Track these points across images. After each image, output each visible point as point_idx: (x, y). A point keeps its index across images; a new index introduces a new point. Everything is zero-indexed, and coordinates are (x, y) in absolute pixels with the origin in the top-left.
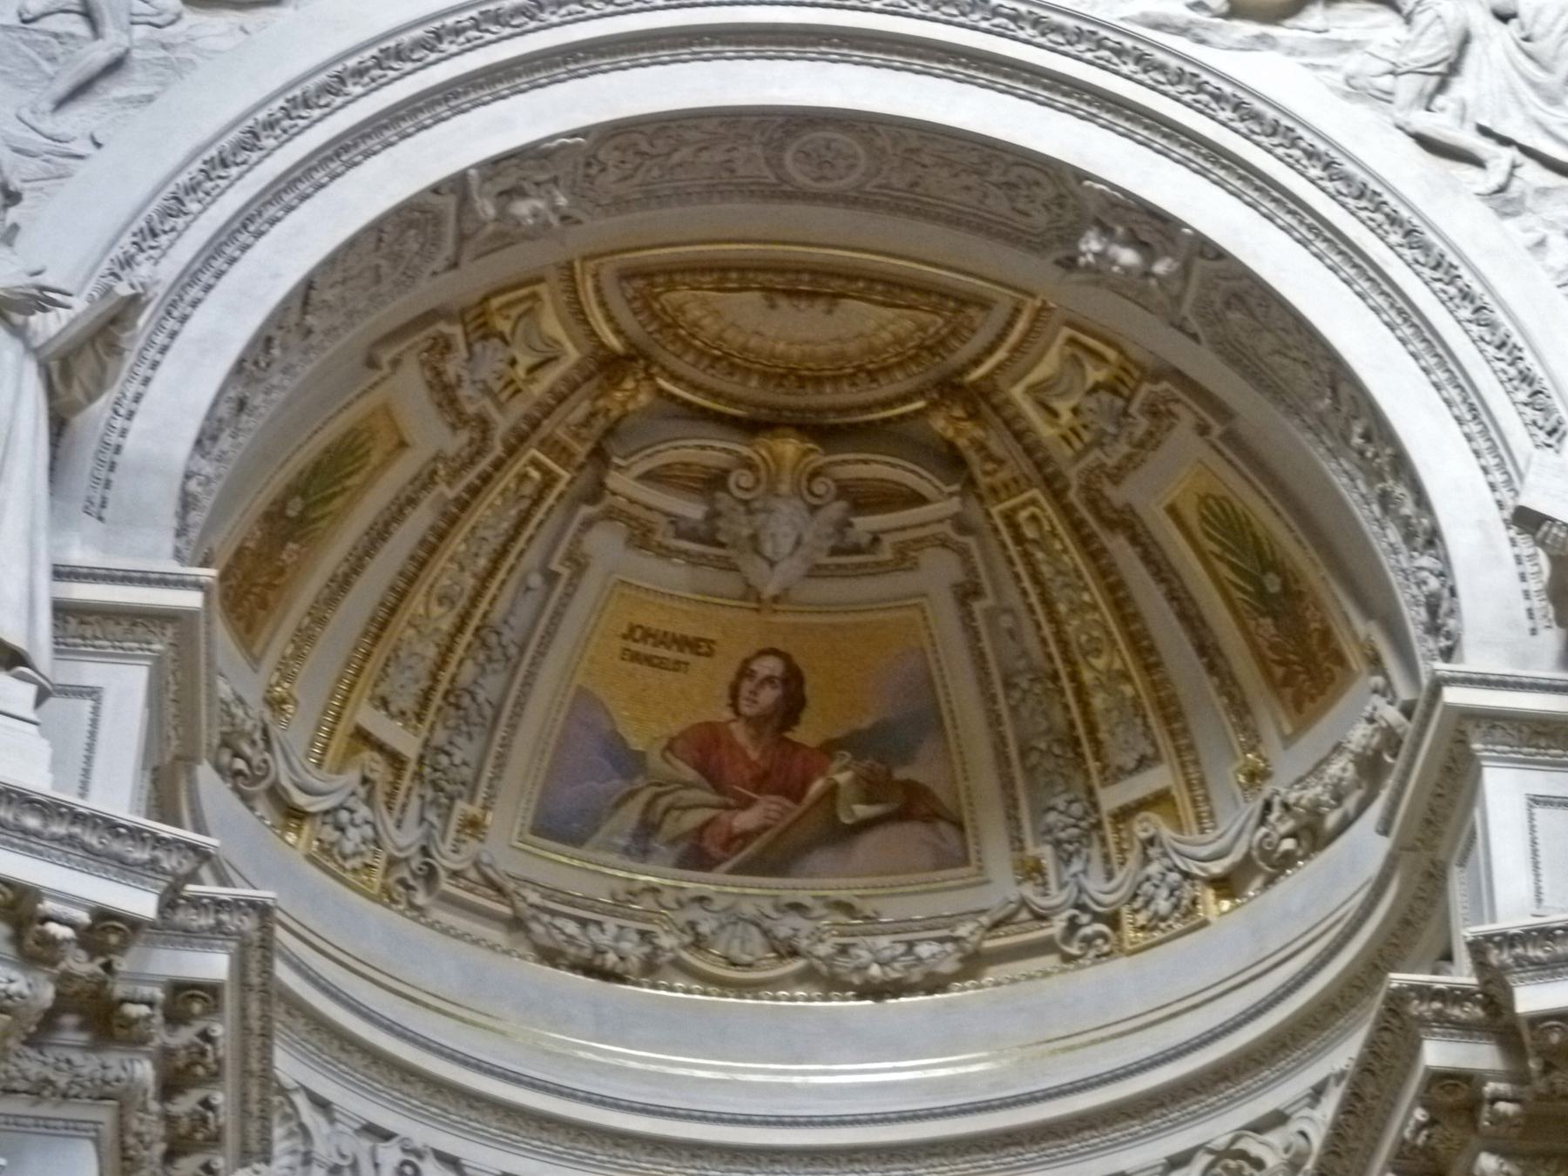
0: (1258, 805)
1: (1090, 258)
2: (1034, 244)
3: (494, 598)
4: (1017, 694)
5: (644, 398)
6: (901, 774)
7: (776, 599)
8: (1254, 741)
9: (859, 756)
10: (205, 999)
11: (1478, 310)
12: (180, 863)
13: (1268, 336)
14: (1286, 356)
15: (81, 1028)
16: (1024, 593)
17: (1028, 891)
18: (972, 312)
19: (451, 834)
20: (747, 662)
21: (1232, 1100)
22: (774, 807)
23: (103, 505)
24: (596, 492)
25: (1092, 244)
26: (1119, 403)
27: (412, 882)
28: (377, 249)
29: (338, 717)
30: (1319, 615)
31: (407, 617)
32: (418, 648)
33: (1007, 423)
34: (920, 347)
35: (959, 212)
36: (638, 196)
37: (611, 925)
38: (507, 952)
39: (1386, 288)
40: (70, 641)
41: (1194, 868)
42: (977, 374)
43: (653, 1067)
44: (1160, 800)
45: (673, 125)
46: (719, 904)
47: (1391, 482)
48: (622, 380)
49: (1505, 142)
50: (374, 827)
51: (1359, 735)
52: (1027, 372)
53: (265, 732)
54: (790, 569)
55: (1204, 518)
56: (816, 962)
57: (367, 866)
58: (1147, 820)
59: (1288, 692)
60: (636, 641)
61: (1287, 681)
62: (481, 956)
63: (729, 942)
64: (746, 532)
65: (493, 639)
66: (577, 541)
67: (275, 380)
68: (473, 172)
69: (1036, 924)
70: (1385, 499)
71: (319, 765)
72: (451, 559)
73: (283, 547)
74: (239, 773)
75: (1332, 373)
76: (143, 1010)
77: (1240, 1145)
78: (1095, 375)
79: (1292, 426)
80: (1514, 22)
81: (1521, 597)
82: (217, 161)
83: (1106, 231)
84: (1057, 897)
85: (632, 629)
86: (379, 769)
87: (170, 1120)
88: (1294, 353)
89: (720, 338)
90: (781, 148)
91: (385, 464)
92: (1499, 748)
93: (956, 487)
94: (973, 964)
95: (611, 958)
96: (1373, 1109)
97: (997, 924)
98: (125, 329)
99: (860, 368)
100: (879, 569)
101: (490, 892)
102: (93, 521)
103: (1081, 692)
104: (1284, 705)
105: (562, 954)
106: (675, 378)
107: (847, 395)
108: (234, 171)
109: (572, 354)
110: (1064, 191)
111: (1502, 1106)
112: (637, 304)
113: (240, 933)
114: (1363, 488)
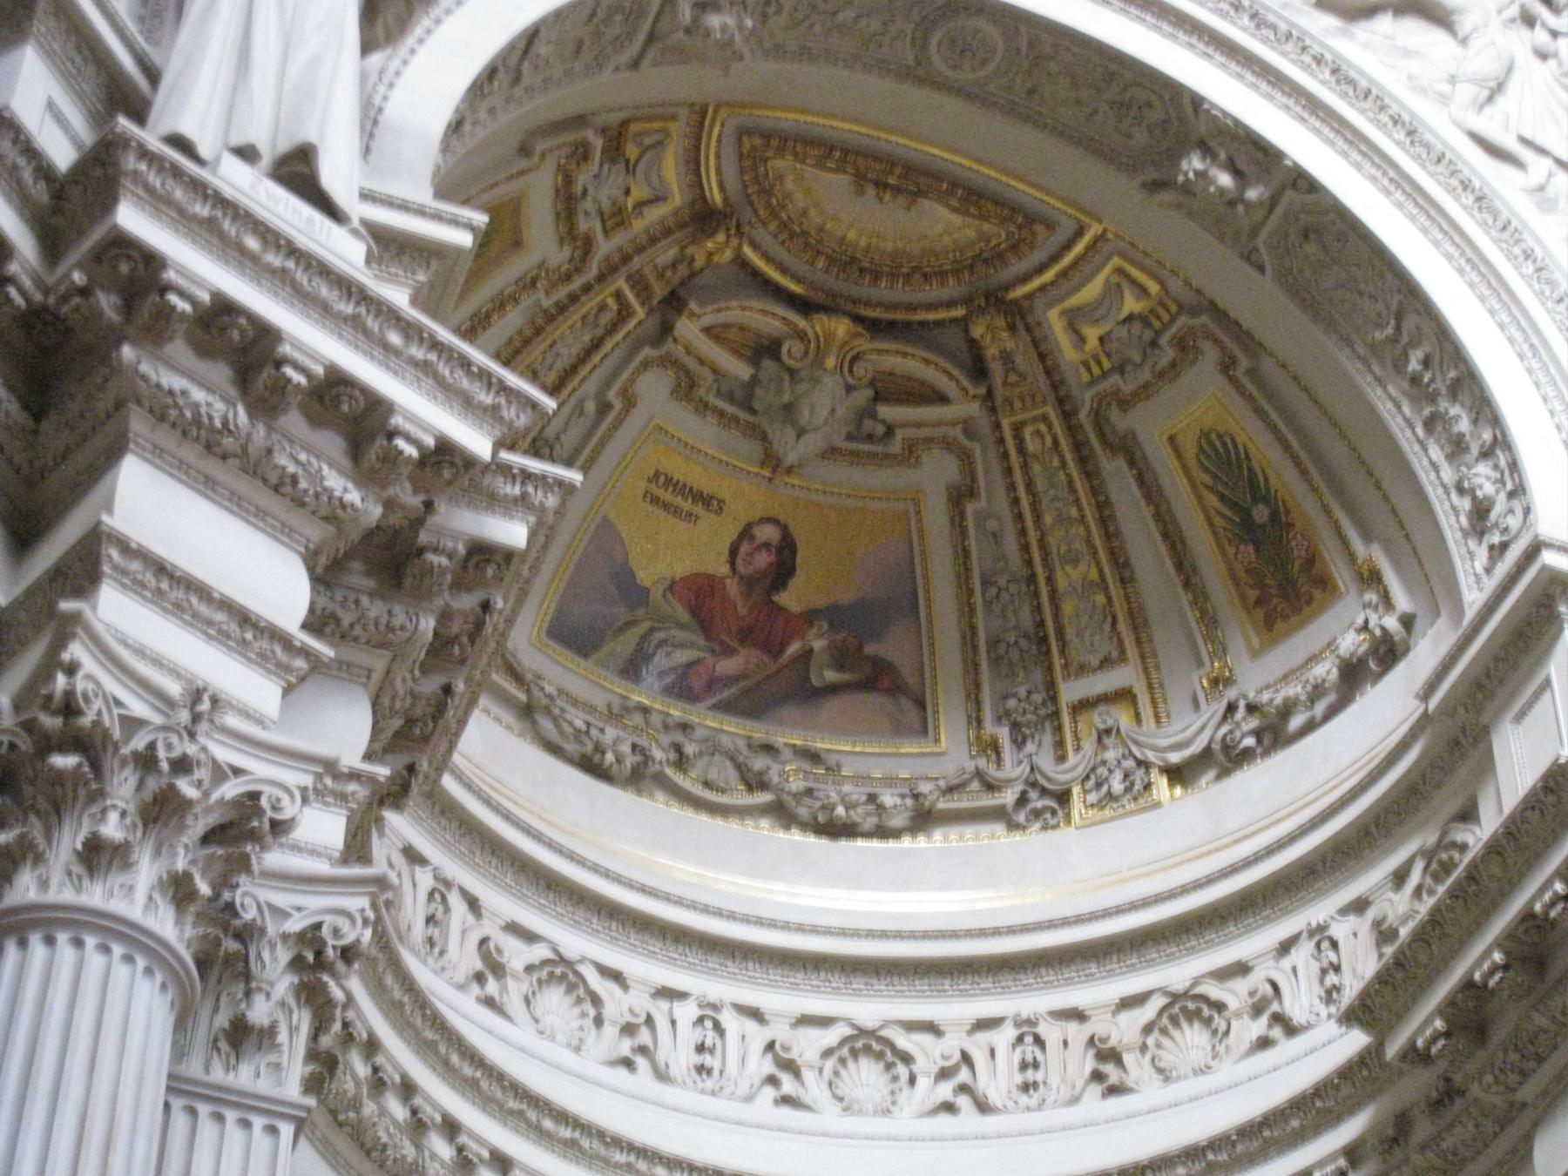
4: (993, 591)
5: (728, 255)
6: (870, 649)
8: (1221, 651)
11: (1539, 270)
15: (368, 573)
16: (1016, 501)
18: (1039, 228)
24: (666, 329)
25: (1195, 163)
33: (1035, 343)
41: (1151, 756)
42: (1020, 291)
48: (715, 231)
49: (1542, 151)
51: (1350, 643)
52: (1069, 294)
54: (812, 443)
56: (785, 796)
59: (1260, 613)
66: (632, 381)
76: (444, 561)
77: (1199, 990)
78: (1131, 304)
79: (1343, 356)
80: (1552, 63)
83: (1207, 150)
85: (657, 474)
94: (923, 819)
97: (950, 790)
99: (915, 269)
100: (887, 459)
106: (755, 246)
113: (542, 509)
114: (1407, 410)
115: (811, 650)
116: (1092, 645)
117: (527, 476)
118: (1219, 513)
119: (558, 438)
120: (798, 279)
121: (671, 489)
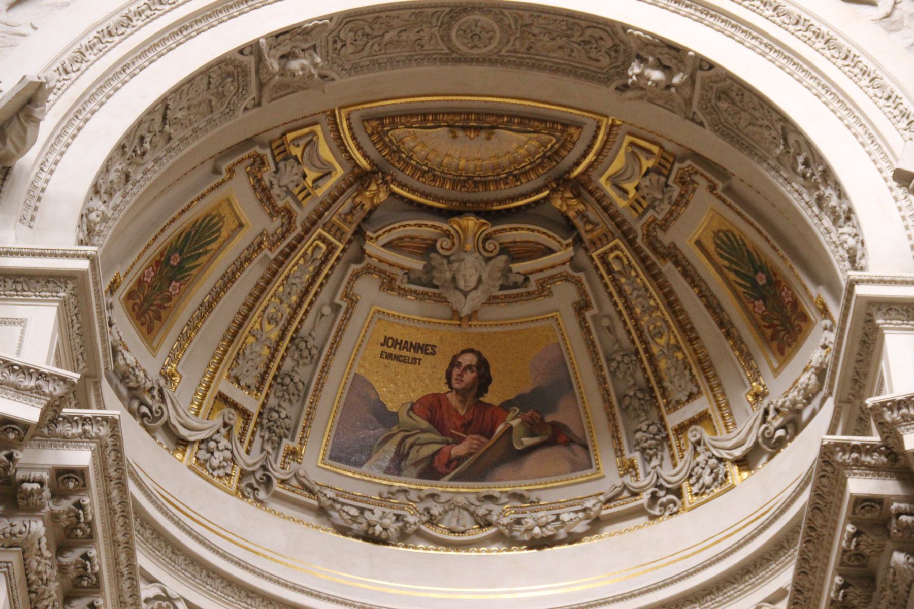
0: (761, 412)
1: (634, 78)
2: (603, 79)
3: (302, 321)
4: (614, 364)
5: (383, 196)
6: (549, 419)
7: (470, 317)
8: (756, 375)
9: (524, 409)
10: (76, 480)
12: (55, 389)
13: (743, 114)
14: (754, 125)
16: (615, 304)
17: (628, 479)
18: (572, 130)
19: (280, 458)
20: (455, 357)
21: (754, 585)
22: (476, 442)
23: (33, 219)
25: (635, 69)
26: (663, 179)
27: (256, 486)
28: (209, 88)
29: (208, 387)
30: (790, 293)
31: (248, 329)
32: (257, 348)
33: (599, 201)
34: (544, 157)
35: (558, 64)
36: (368, 63)
37: (378, 511)
38: (317, 528)
39: (814, 74)
40: (7, 293)
41: (724, 454)
43: (405, 592)
44: (703, 418)
45: (383, 15)
46: (443, 498)
47: (822, 188)
48: (368, 186)
50: (232, 452)
53: (161, 391)
54: (477, 298)
55: (717, 245)
57: (227, 475)
58: (695, 430)
59: (775, 344)
60: (388, 346)
61: (773, 338)
62: (300, 528)
63: (450, 520)
64: (449, 275)
65: (303, 345)
67: (150, 166)
68: (262, 41)
69: (633, 499)
70: (820, 201)
71: (197, 414)
72: (274, 295)
73: (170, 284)
74: (144, 415)
75: (783, 129)
78: (647, 164)
79: (762, 169)
81: (906, 238)
82: (105, 32)
83: (642, 60)
84: (644, 481)
85: (386, 340)
86: (237, 422)
87: (62, 569)
88: (760, 122)
89: (426, 159)
90: (449, 28)
91: (230, 238)
92: (894, 322)
93: (570, 240)
94: (597, 524)
95: (378, 529)
96: (823, 535)
97: (609, 501)
98: (37, 106)
99: (510, 173)
100: (530, 296)
101: (305, 493)
102: (26, 228)
103: (652, 359)
104: (773, 352)
105: (351, 529)
106: (402, 185)
107: (505, 191)
108: (117, 39)
109: (339, 172)
110: (617, 41)
111: (904, 518)
112: (375, 138)
114: (805, 196)
115: (511, 427)
116: (681, 386)
117: (85, 420)
118: (739, 284)
119: (310, 335)
120: (436, 199)
121: (398, 346)
